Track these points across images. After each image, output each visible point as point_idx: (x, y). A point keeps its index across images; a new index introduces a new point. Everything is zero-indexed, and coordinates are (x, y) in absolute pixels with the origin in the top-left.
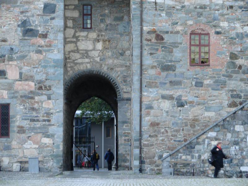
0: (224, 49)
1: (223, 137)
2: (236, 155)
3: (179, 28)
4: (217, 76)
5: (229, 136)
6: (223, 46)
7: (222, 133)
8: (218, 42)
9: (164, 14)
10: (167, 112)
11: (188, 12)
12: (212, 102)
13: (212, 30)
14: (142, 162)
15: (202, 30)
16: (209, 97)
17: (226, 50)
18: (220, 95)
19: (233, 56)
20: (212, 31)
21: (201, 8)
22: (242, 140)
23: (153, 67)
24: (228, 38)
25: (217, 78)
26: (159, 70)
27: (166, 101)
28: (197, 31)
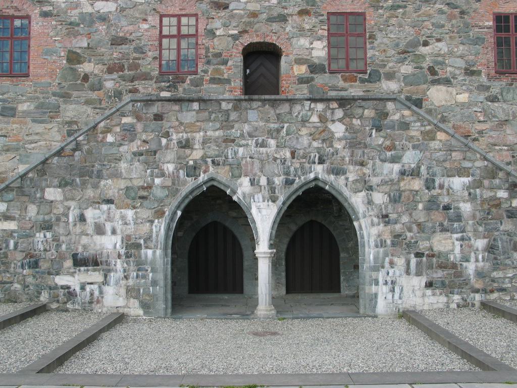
0: (57, 44)
1: (19, 212)
2: (45, 250)
4: (41, 96)
5: (32, 210)
6: (54, 39)
7: (18, 203)
8: (46, 31)
12: (33, 145)
13: (35, 10)
16: (27, 135)
17: (60, 45)
18: (47, 131)
20: (35, 12)
22: (58, 219)
24: (64, 23)
25: (42, 100)
28: (7, 11)
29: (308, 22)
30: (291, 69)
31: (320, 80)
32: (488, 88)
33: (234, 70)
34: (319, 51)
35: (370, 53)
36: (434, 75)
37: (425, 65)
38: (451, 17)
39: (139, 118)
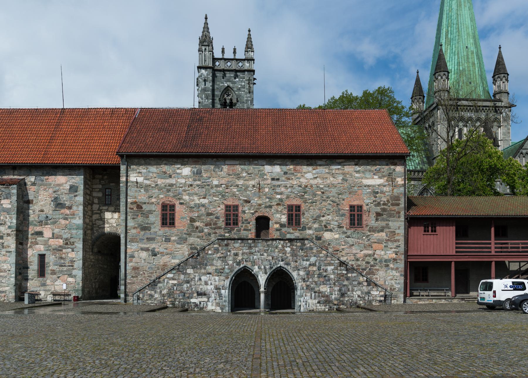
3: (153, 200)
9: (142, 191)
10: (145, 260)
11: (160, 189)
14: (126, 295)
15: (170, 201)
19: (192, 220)
21: (169, 186)
23: (134, 228)
26: (139, 230)
27: (144, 252)
29: (280, 208)
30: (273, 226)
31: (284, 230)
32: (346, 233)
33: (252, 226)
34: (284, 219)
35: (302, 220)
36: (326, 228)
37: (323, 224)
38: (333, 206)
39: (220, 245)
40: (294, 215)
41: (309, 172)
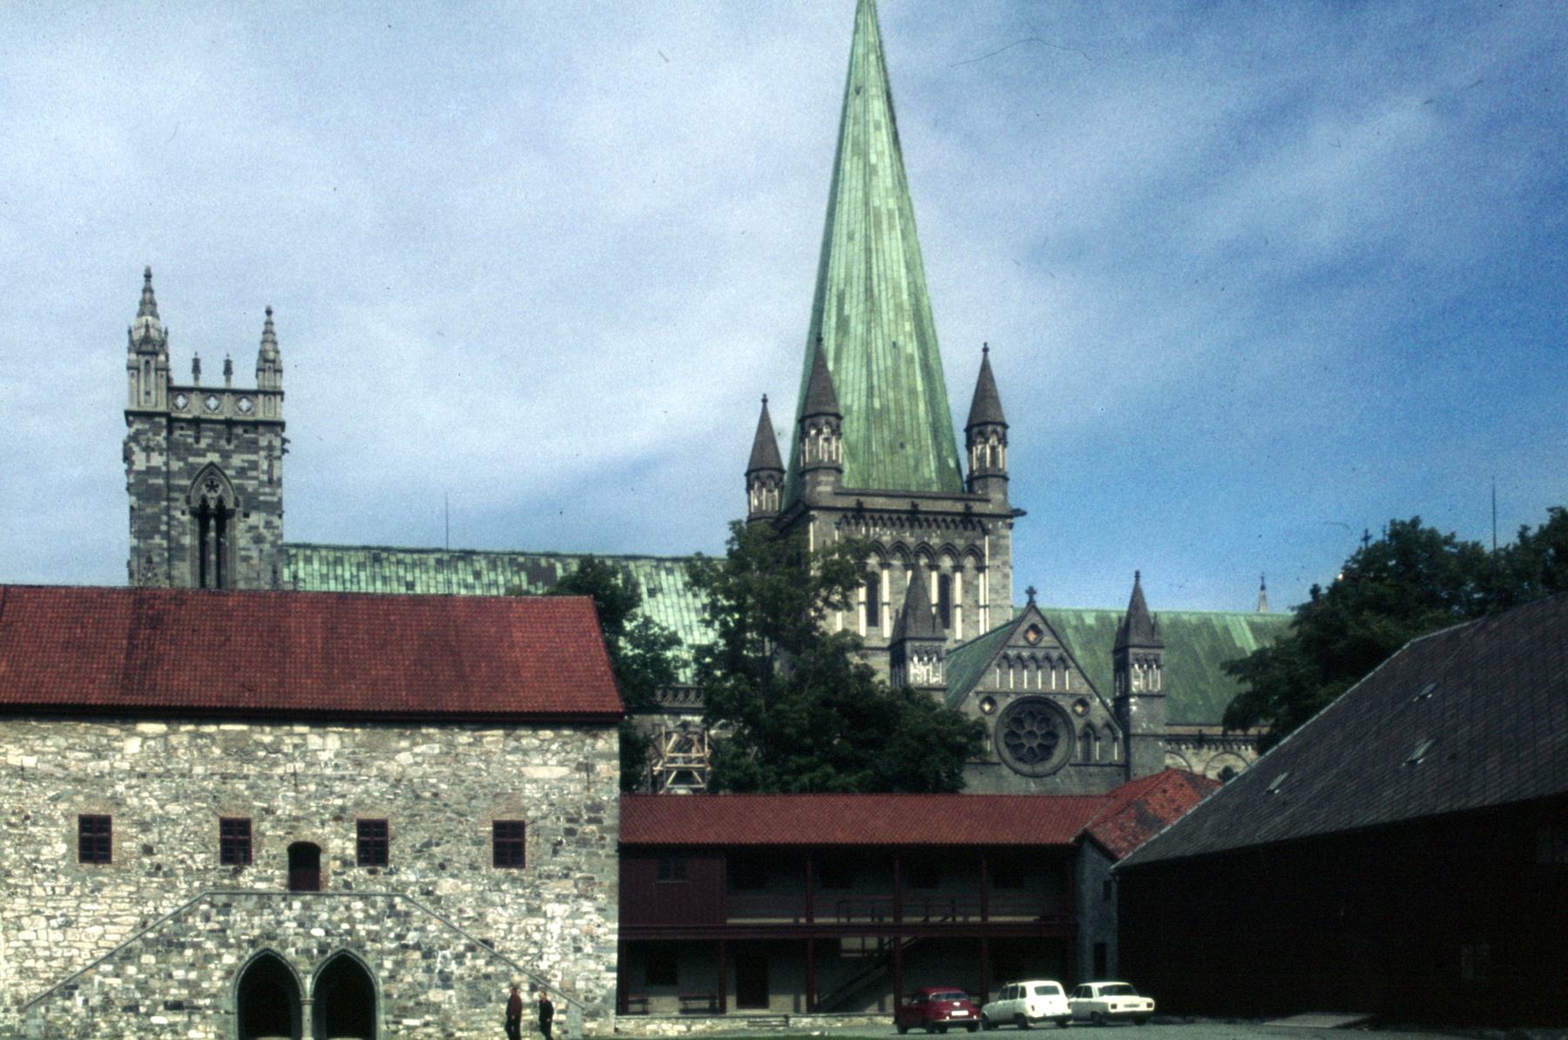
30: (329, 866)
34: (351, 850)
40: (374, 844)
41: (404, 750)
